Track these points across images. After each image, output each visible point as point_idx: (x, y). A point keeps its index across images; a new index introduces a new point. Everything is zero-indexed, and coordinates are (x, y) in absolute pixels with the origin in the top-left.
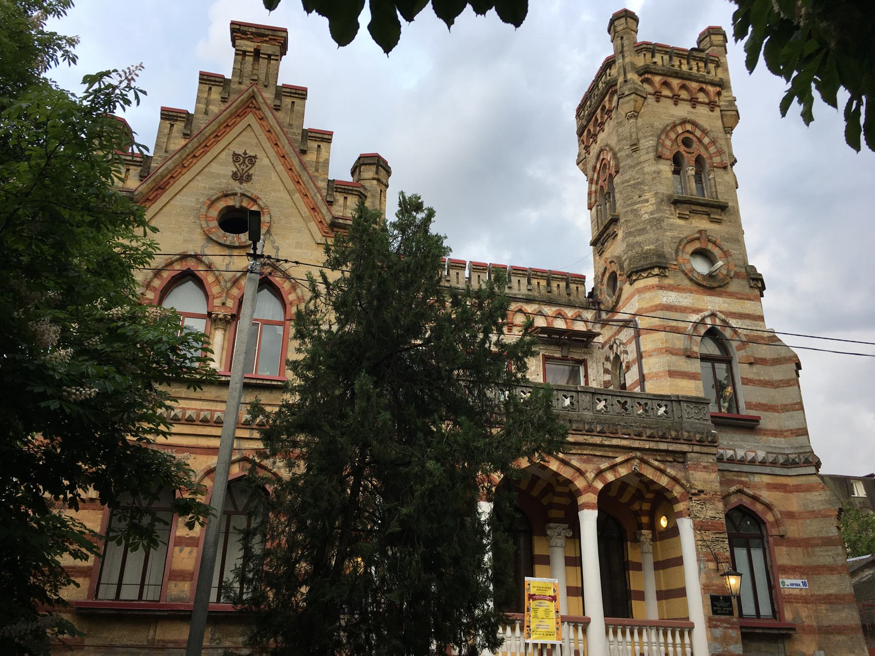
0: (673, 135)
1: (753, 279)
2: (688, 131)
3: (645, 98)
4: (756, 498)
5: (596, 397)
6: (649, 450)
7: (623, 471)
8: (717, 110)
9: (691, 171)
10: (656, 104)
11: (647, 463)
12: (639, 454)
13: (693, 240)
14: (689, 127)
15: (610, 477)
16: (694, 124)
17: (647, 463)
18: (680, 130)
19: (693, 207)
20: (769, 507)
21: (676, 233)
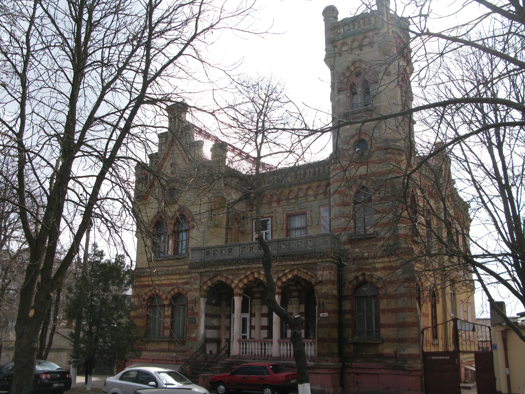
0: (348, 74)
1: (385, 149)
2: (358, 67)
3: (335, 57)
4: (372, 276)
5: (280, 243)
6: (299, 264)
7: (290, 276)
8: (376, 46)
9: (359, 90)
10: (340, 58)
11: (300, 270)
12: (295, 267)
13: (353, 136)
14: (357, 65)
15: (284, 280)
16: (360, 61)
17: (300, 270)
18: (352, 69)
19: (355, 116)
20: (379, 279)
21: (346, 134)
